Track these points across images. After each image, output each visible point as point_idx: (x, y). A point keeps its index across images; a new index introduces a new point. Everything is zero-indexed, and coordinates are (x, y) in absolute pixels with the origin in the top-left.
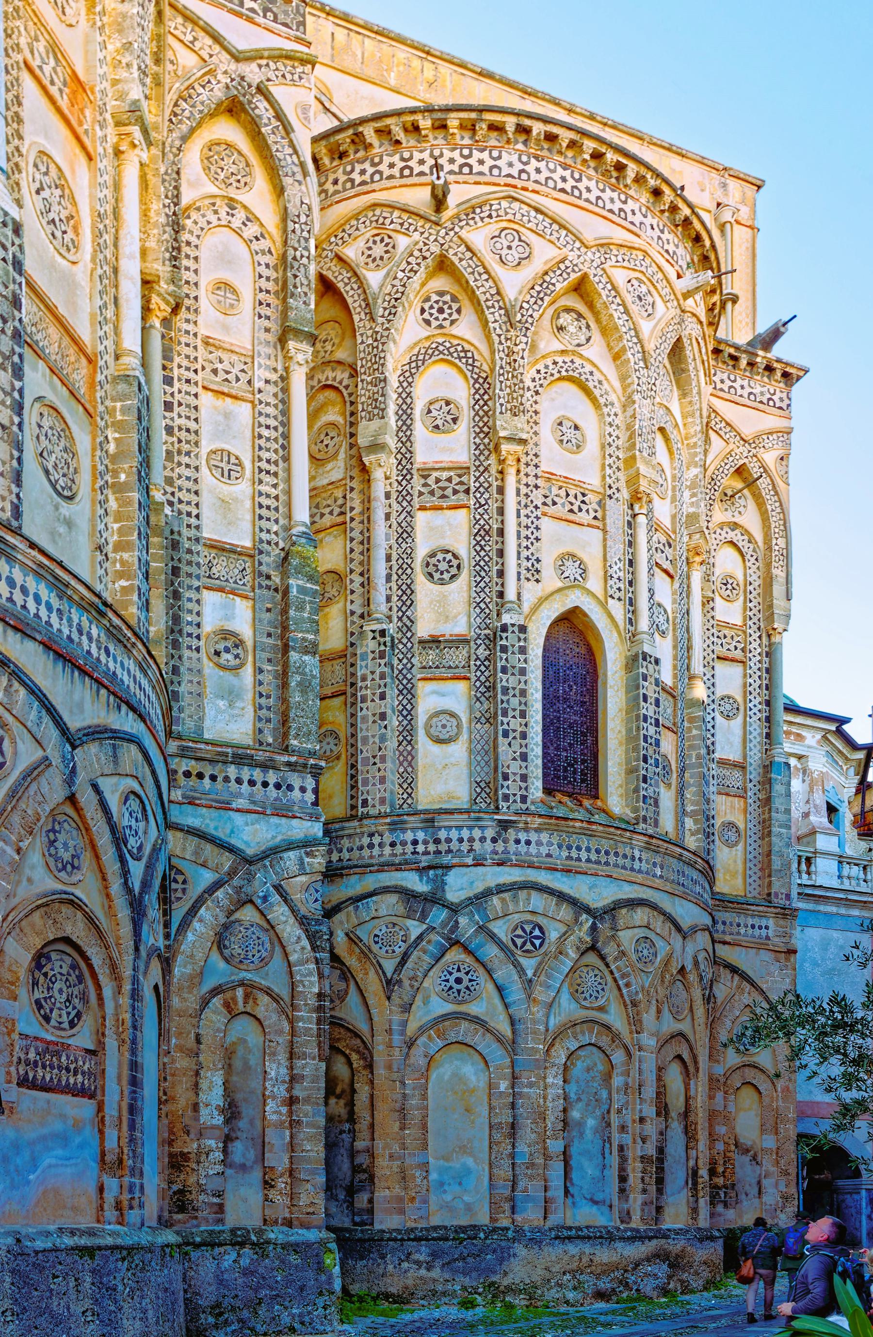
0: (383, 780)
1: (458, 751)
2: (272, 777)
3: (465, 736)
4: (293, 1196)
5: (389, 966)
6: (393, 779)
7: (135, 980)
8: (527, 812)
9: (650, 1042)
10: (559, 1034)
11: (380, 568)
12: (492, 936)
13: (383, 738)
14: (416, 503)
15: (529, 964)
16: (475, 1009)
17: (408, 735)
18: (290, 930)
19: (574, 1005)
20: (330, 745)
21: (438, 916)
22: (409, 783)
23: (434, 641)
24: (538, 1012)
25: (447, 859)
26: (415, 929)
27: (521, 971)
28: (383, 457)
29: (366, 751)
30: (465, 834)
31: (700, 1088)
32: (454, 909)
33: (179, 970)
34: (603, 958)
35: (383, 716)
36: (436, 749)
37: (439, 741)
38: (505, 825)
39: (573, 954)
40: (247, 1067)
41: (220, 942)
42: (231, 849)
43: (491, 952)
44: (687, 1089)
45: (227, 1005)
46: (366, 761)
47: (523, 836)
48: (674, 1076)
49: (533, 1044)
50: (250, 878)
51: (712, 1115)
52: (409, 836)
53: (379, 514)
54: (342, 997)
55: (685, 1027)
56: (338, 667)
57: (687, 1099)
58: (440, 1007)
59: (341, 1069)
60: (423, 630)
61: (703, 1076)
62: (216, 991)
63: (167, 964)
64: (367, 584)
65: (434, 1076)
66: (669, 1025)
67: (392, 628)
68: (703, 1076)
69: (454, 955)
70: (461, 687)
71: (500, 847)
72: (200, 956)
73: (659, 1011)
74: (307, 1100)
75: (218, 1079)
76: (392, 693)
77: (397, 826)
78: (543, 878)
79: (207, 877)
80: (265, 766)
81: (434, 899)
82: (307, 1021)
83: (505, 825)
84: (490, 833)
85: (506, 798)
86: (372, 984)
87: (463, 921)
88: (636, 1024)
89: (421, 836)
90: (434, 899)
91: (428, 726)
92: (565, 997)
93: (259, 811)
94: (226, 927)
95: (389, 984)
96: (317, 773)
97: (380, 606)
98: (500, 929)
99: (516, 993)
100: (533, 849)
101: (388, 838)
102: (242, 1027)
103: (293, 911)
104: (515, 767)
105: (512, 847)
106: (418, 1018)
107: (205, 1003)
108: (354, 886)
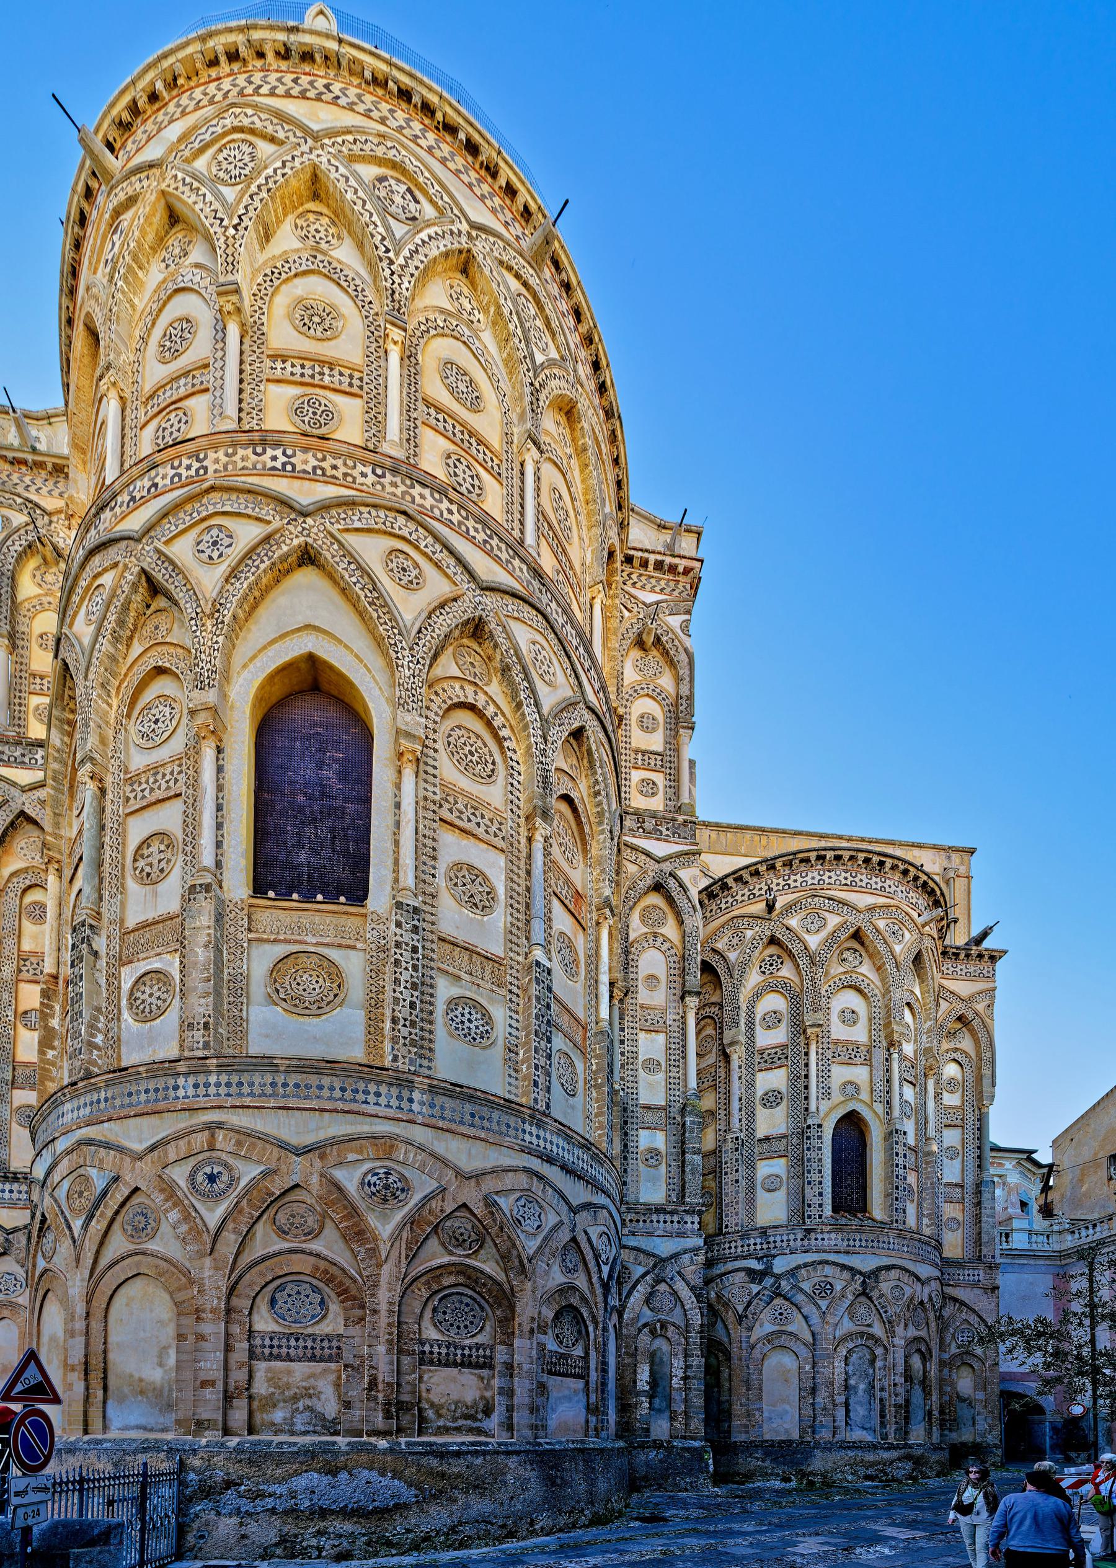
0: (737, 1214)
1: (781, 1195)
2: (676, 1218)
3: (784, 1187)
4: (687, 1425)
5: (740, 1308)
6: (742, 1213)
7: (604, 1322)
8: (823, 1224)
9: (899, 1342)
10: (844, 1339)
11: (735, 1105)
12: (801, 1290)
13: (737, 1192)
14: (756, 1068)
15: (823, 1304)
16: (789, 1328)
17: (751, 1189)
18: (685, 1293)
19: (851, 1324)
20: (707, 1199)
21: (769, 1281)
22: (751, 1214)
23: (767, 1139)
24: (829, 1329)
25: (774, 1252)
26: (755, 1288)
27: (819, 1307)
28: (737, 1047)
29: (726, 1200)
30: (785, 1238)
31: (933, 1368)
32: (778, 1277)
33: (626, 1316)
34: (870, 1298)
35: (737, 1181)
36: (768, 1195)
37: (770, 1191)
38: (809, 1231)
39: (851, 1297)
40: (661, 1361)
41: (647, 1301)
42: (654, 1255)
43: (800, 1298)
44: (924, 1367)
45: (651, 1332)
46: (727, 1205)
47: (819, 1236)
48: (916, 1362)
49: (826, 1346)
50: (664, 1268)
51: (942, 1382)
52: (752, 1241)
53: (735, 1073)
54: (713, 1324)
55: (923, 1333)
56: (711, 1158)
57: (925, 1372)
58: (769, 1328)
59: (713, 1361)
60: (760, 1133)
61: (935, 1360)
62: (645, 1325)
63: (620, 1316)
64: (728, 1114)
65: (766, 1363)
66: (912, 1332)
67: (742, 1135)
68: (935, 1360)
69: (778, 1301)
70: (783, 1161)
71: (806, 1242)
72: (637, 1308)
73: (906, 1325)
74: (694, 1378)
75: (647, 1368)
76: (742, 1169)
77: (745, 1236)
78: (832, 1257)
79: (641, 1270)
80: (672, 1213)
81: (767, 1272)
82: (695, 1339)
83: (809, 1231)
84: (799, 1236)
85: (809, 1217)
86: (730, 1317)
87: (783, 1283)
88: (891, 1333)
89: (759, 1241)
90: (767, 1272)
91: (763, 1183)
92: (846, 1319)
93: (669, 1235)
94: (651, 1294)
95: (741, 1318)
96: (700, 1213)
97: (735, 1124)
98: (806, 1286)
99: (815, 1318)
100: (826, 1243)
101: (739, 1243)
102: (660, 1344)
103: (688, 1284)
104: (815, 1200)
105: (813, 1242)
106: (758, 1333)
107: (640, 1330)
108: (720, 1269)
